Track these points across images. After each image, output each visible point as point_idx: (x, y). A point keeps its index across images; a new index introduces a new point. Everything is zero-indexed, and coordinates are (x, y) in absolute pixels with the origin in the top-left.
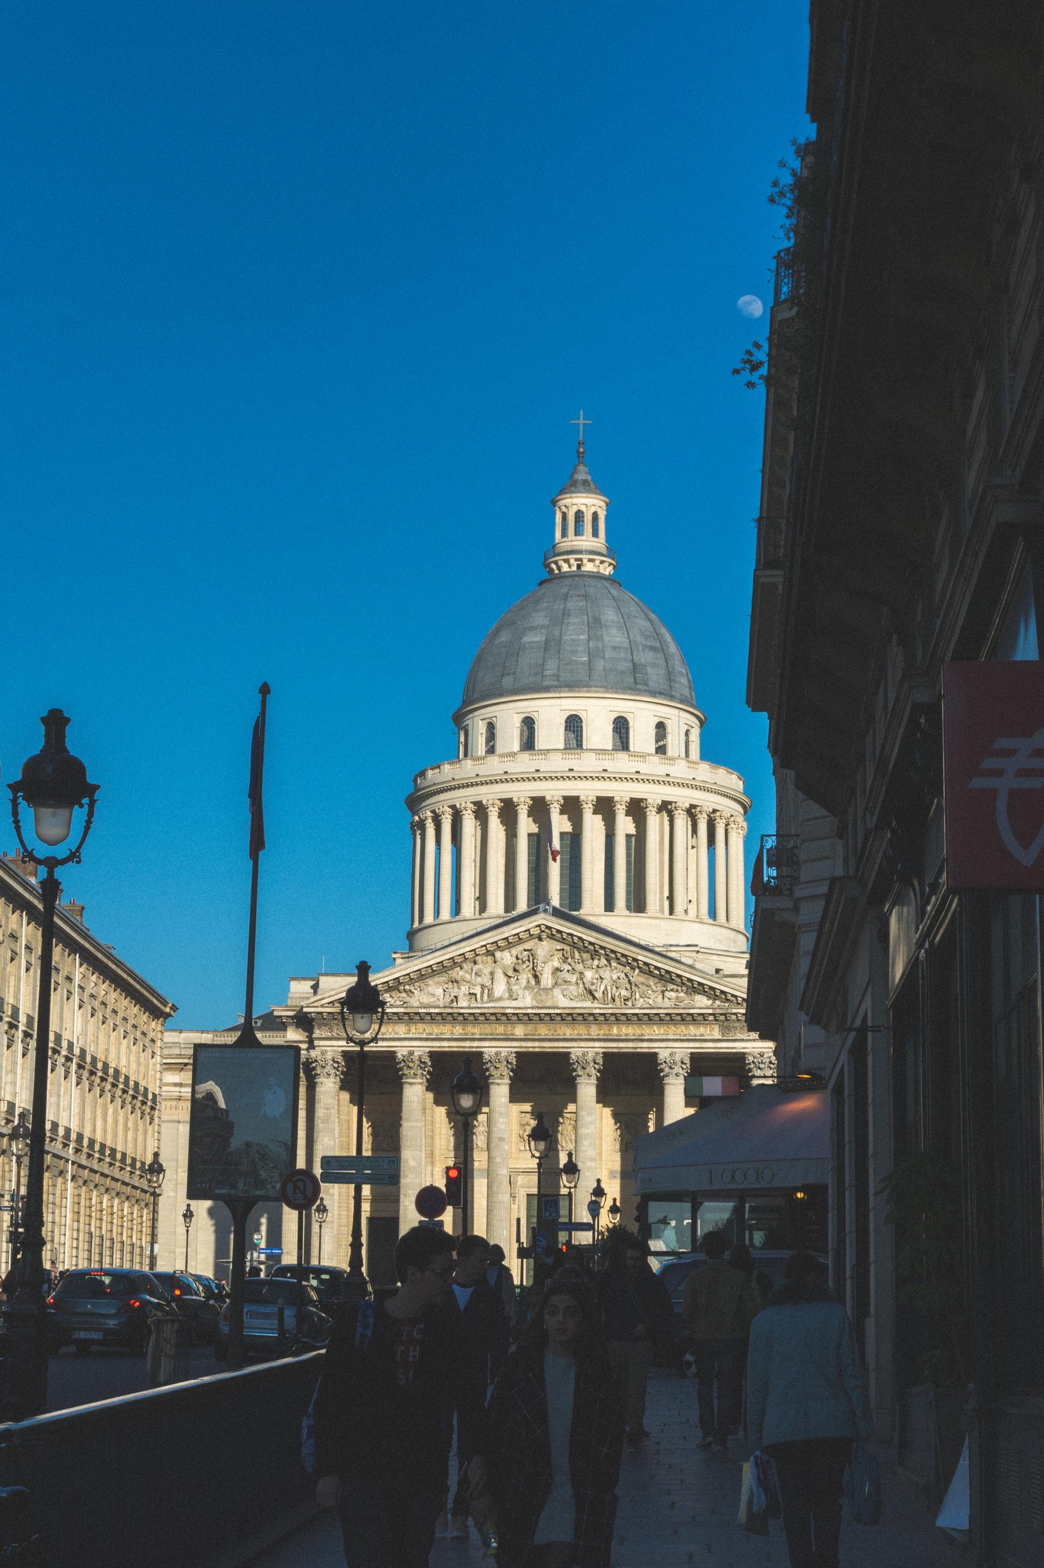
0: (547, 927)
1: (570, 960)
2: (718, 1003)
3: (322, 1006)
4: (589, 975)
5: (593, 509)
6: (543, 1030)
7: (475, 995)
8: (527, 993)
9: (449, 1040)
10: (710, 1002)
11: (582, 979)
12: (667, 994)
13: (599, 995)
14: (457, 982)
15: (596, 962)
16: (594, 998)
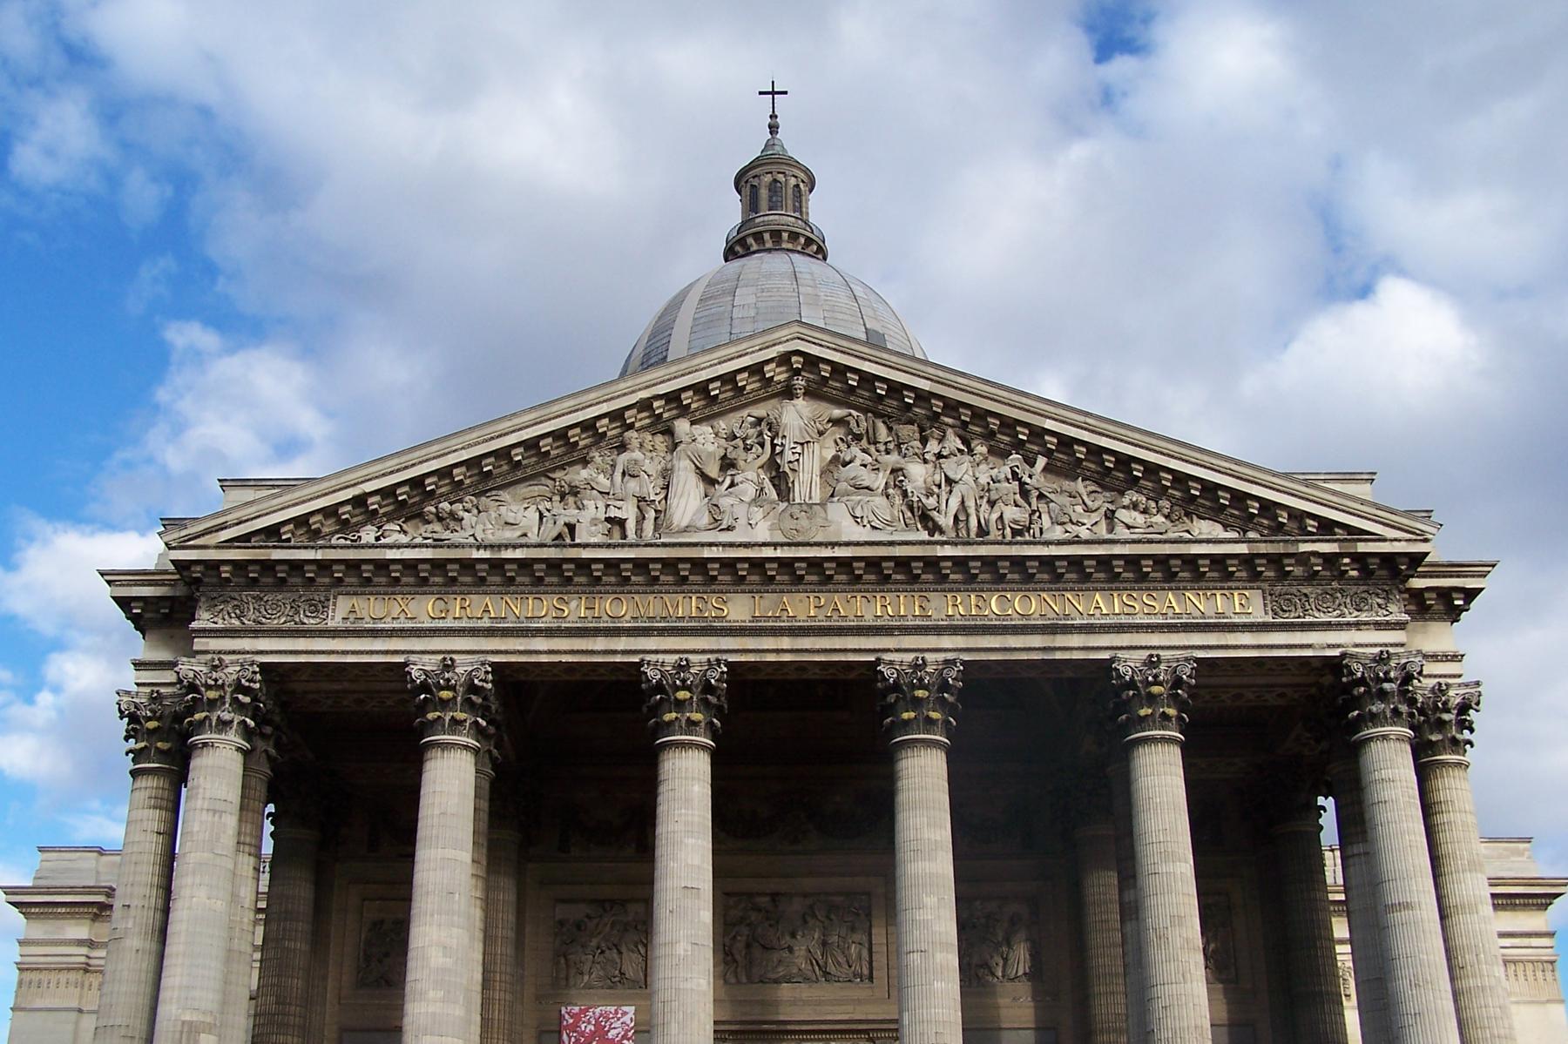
0: (812, 362)
1: (864, 442)
2: (1251, 535)
3: (218, 547)
4: (918, 473)
5: (793, 181)
6: (802, 607)
7: (621, 523)
8: (758, 513)
9: (549, 633)
10: (1234, 535)
11: (898, 485)
12: (1123, 515)
13: (945, 521)
14: (575, 491)
15: (933, 447)
16: (934, 528)
